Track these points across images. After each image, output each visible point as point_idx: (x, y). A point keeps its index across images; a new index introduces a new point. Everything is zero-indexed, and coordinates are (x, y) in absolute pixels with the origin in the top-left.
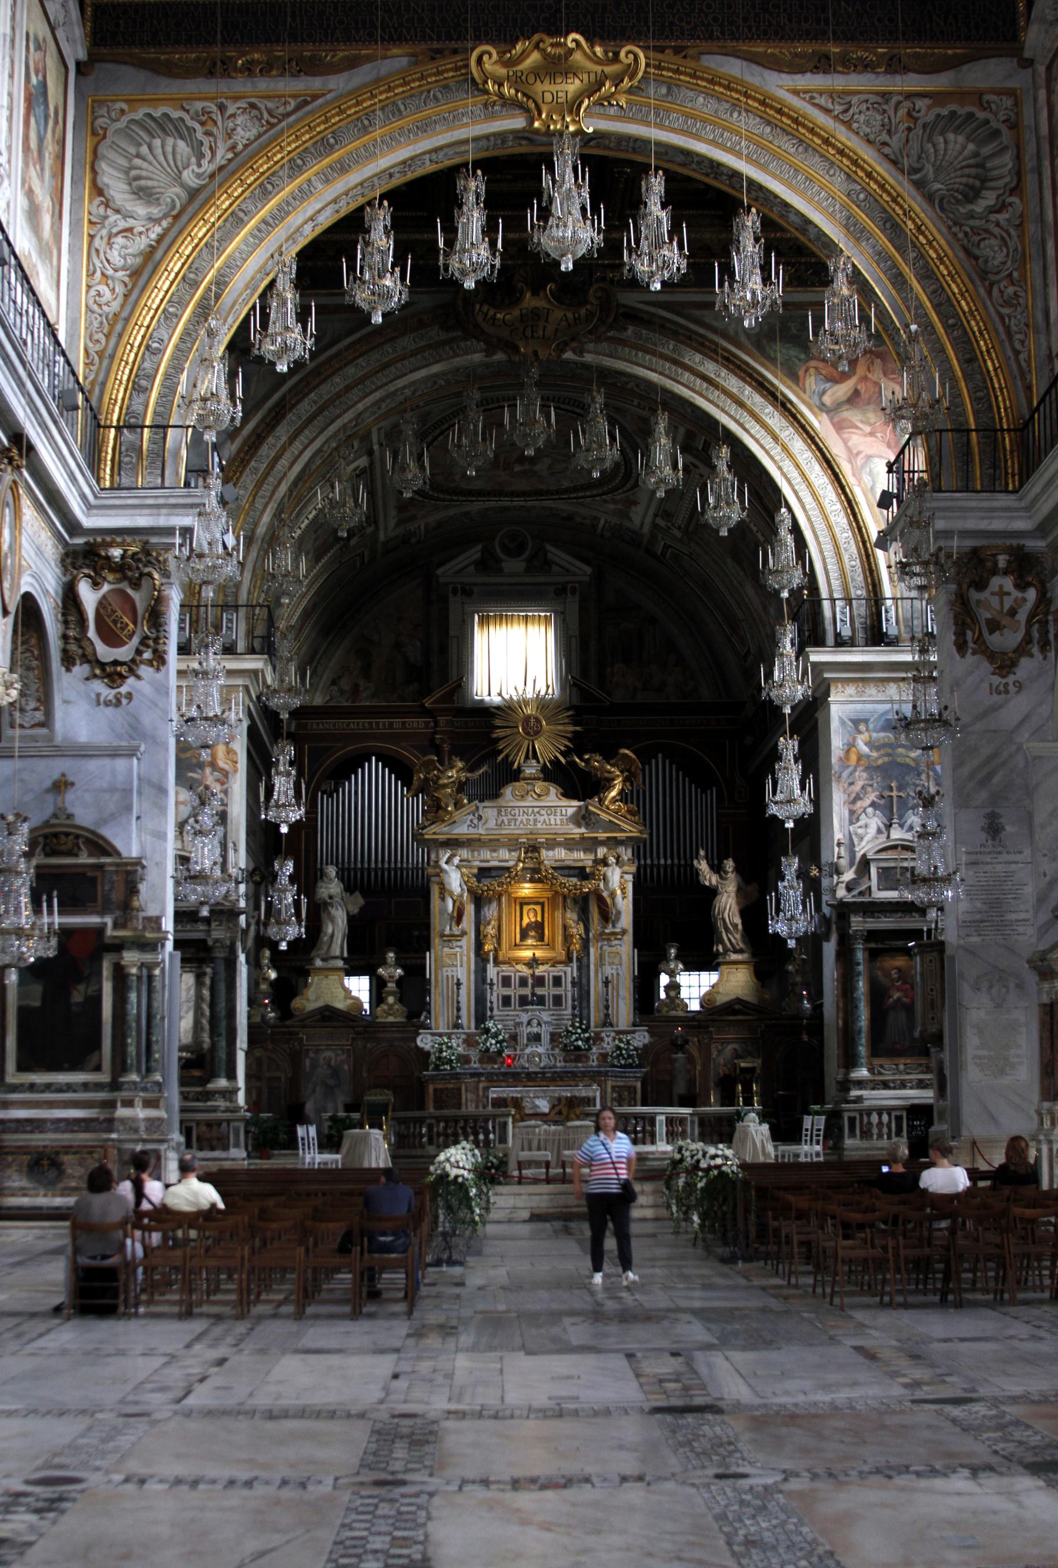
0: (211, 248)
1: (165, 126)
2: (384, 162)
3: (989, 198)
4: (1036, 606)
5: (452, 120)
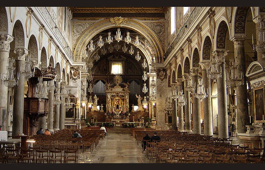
1: (80, 25)
2: (101, 29)
3: (161, 33)
4: (165, 75)
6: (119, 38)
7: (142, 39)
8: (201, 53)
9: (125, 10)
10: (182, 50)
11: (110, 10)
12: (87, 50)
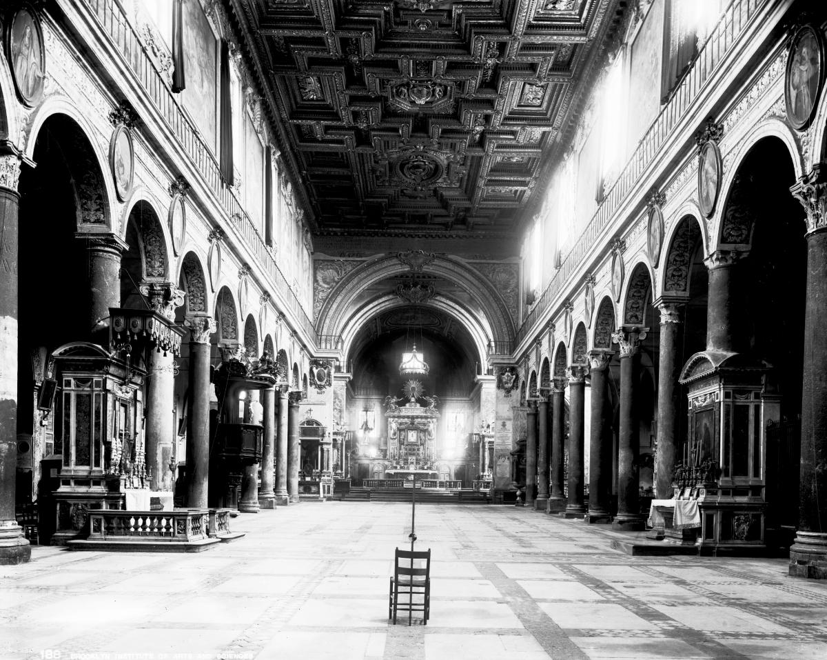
8: (590, 333)
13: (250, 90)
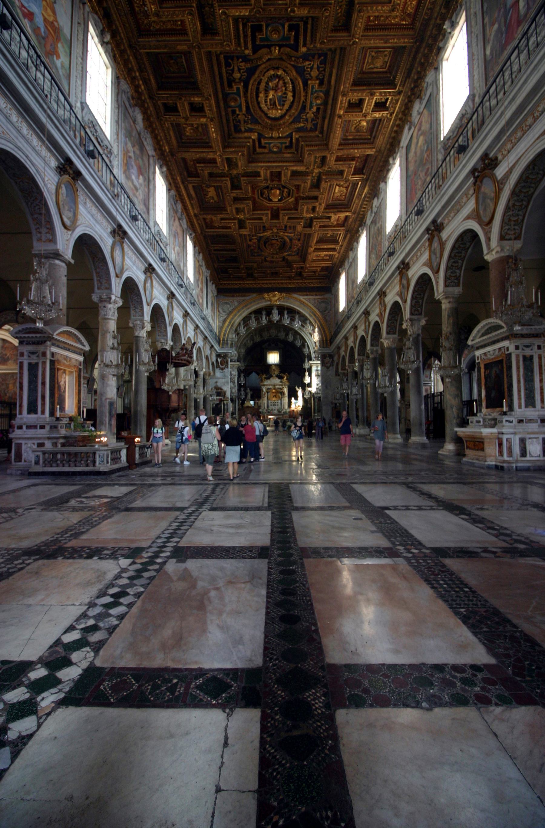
0: (233, 318)
1: (227, 303)
5: (262, 302)
6: (276, 317)
7: (304, 320)
9: (282, 283)
10: (355, 327)
11: (263, 284)
12: (238, 334)
13: (173, 192)
